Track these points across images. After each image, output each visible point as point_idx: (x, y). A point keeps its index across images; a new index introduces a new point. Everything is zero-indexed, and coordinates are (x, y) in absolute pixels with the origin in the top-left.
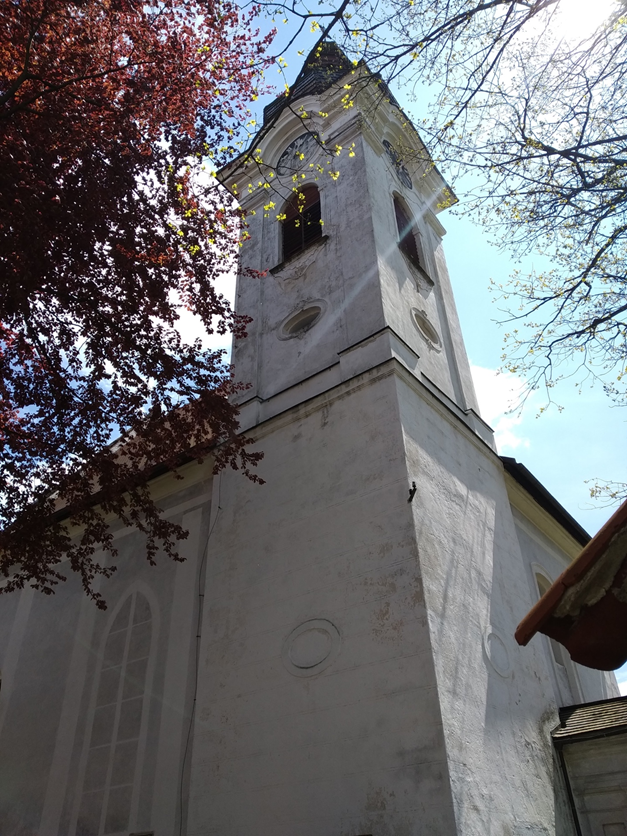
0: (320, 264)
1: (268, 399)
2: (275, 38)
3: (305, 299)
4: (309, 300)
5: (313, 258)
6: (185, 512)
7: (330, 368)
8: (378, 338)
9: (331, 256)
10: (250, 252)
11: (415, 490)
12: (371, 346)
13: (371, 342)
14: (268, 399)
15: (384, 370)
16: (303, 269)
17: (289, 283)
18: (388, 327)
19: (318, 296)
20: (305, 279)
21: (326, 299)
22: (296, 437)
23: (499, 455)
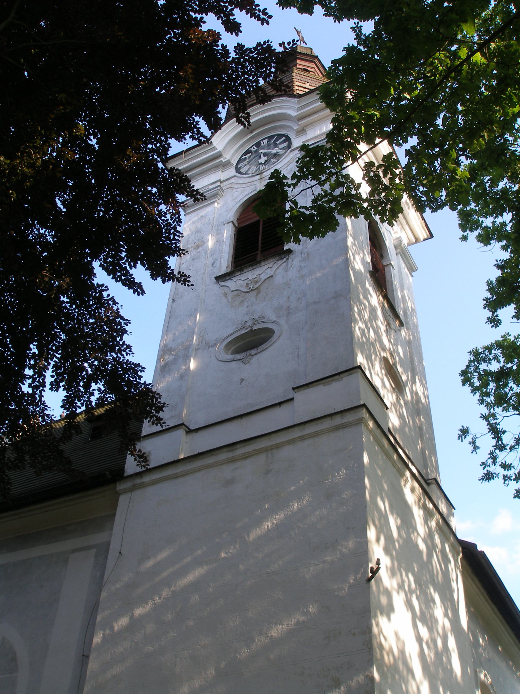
0: (279, 279)
1: (197, 430)
2: (402, 636)
3: (256, 317)
4: (262, 319)
5: (270, 272)
6: (74, 551)
7: (280, 404)
8: (346, 380)
9: (293, 273)
10: (194, 252)
11: (378, 569)
12: (335, 386)
13: (337, 380)
14: (197, 430)
15: (349, 418)
16: (257, 282)
17: (238, 295)
18: (359, 367)
19: (273, 317)
20: (259, 293)
21: (282, 322)
22: (230, 482)
23: (460, 537)
